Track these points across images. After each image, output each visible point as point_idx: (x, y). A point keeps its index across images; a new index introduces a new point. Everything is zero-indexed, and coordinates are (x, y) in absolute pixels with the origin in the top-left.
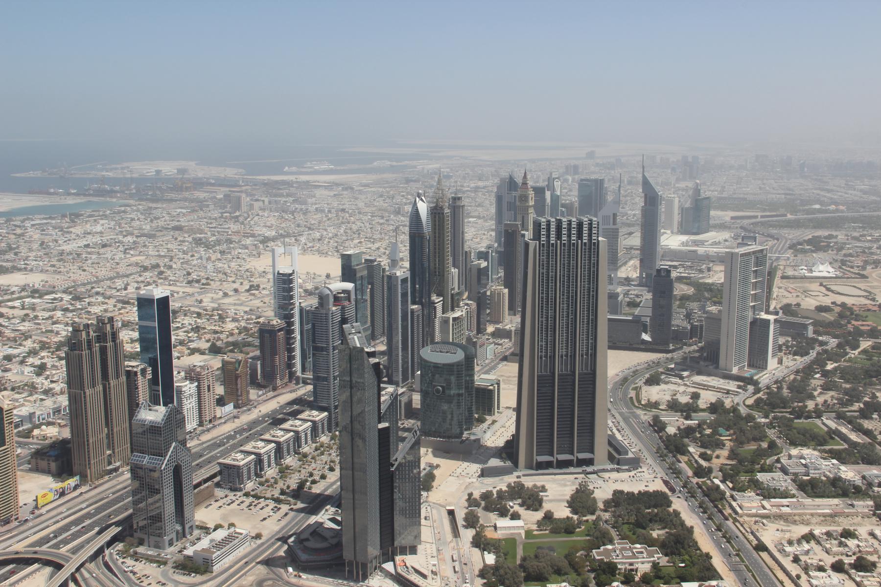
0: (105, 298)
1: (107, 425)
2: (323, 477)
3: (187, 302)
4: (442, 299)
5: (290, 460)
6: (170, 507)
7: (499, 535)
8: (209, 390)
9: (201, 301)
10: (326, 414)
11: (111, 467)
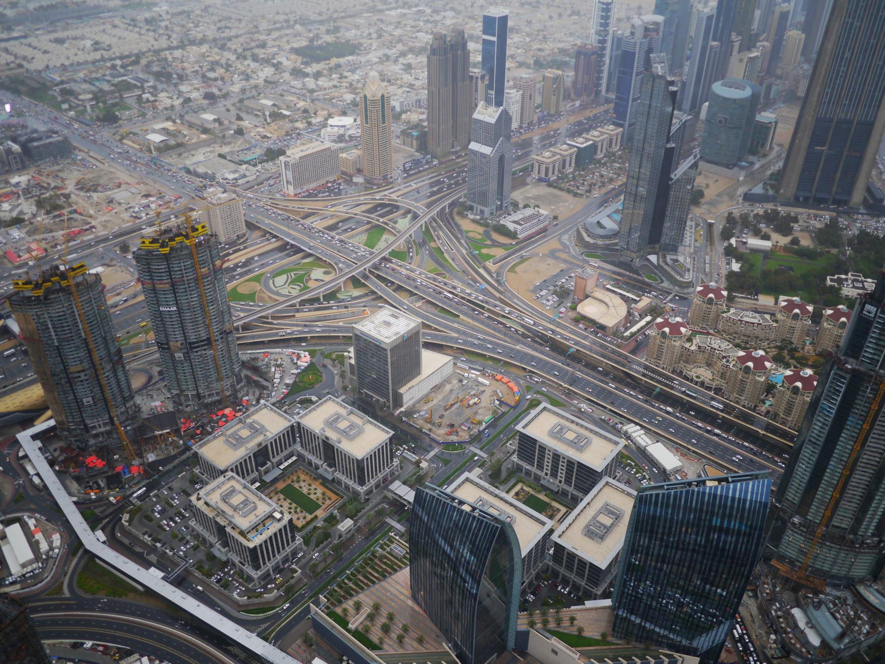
1: (453, 119)
4: (740, 38)
6: (493, 186)
10: (621, 129)
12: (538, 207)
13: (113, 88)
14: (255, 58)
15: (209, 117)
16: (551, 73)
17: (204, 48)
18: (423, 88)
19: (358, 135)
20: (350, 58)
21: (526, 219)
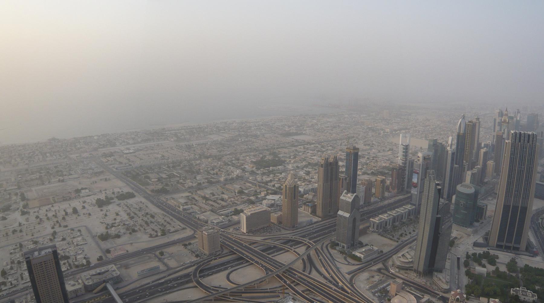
0: (333, 148)
3: (364, 153)
4: (468, 163)
5: (397, 224)
8: (369, 190)
9: (369, 153)
10: (415, 207)
11: (330, 214)
12: (372, 245)
13: (167, 177)
14: (233, 165)
16: (380, 178)
17: (210, 160)
18: (315, 183)
19: (281, 204)
20: (280, 167)
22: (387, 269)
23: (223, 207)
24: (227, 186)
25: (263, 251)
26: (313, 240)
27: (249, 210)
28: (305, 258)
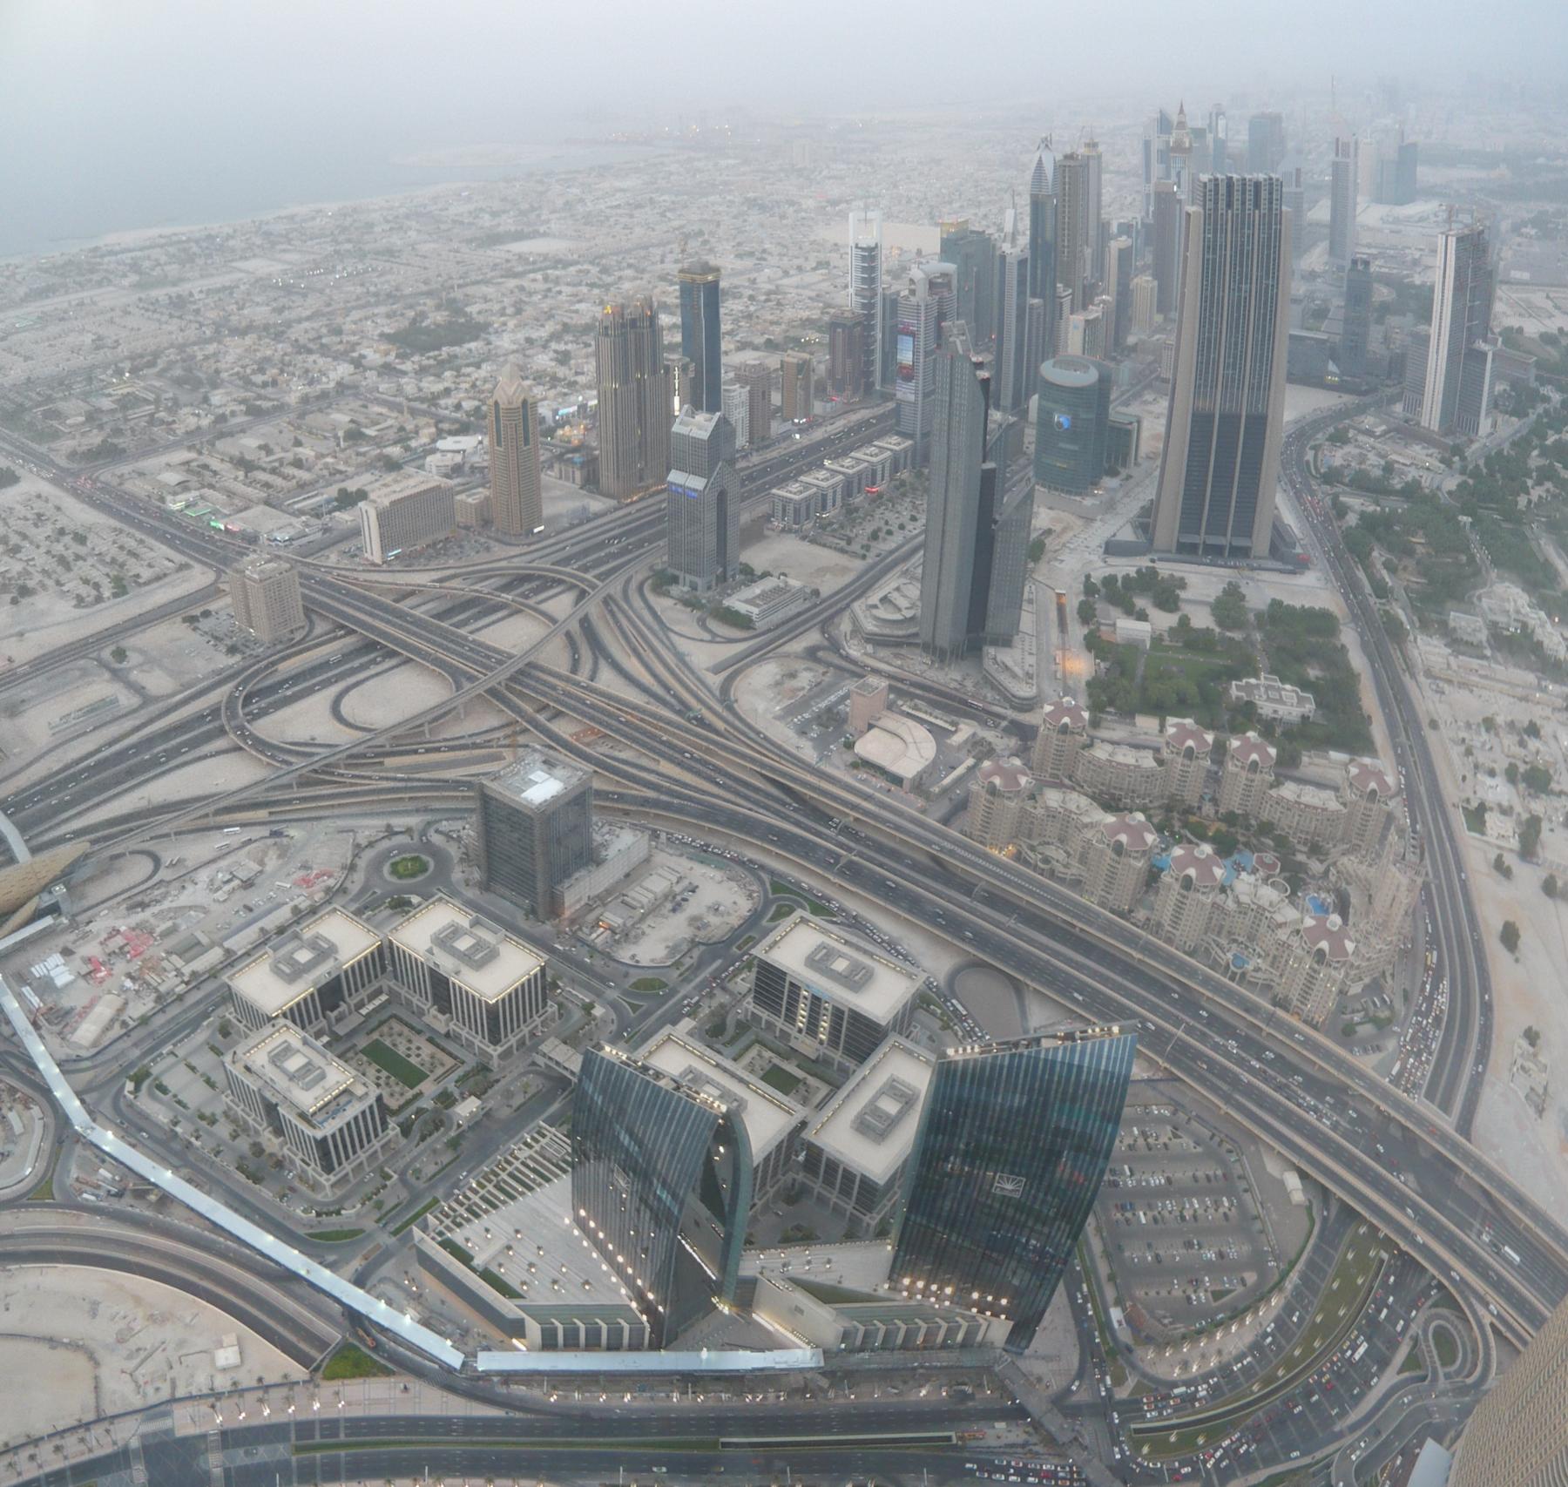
2: (902, 527)
5: (858, 500)
6: (710, 541)
7: (1119, 638)
15: (249, 443)
21: (763, 596)
22: (835, 646)
23: (302, 486)
24: (309, 419)
25: (439, 616)
26: (597, 572)
27: (385, 491)
28: (574, 626)
